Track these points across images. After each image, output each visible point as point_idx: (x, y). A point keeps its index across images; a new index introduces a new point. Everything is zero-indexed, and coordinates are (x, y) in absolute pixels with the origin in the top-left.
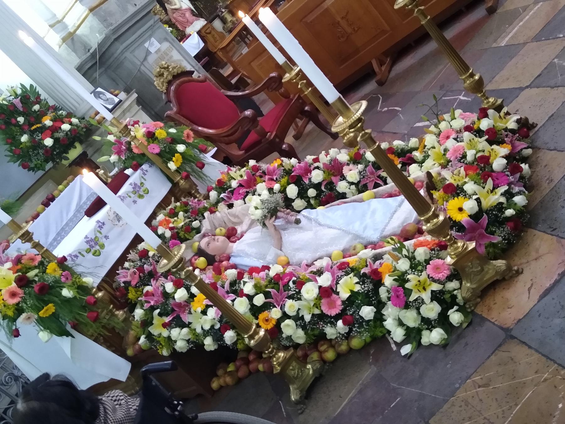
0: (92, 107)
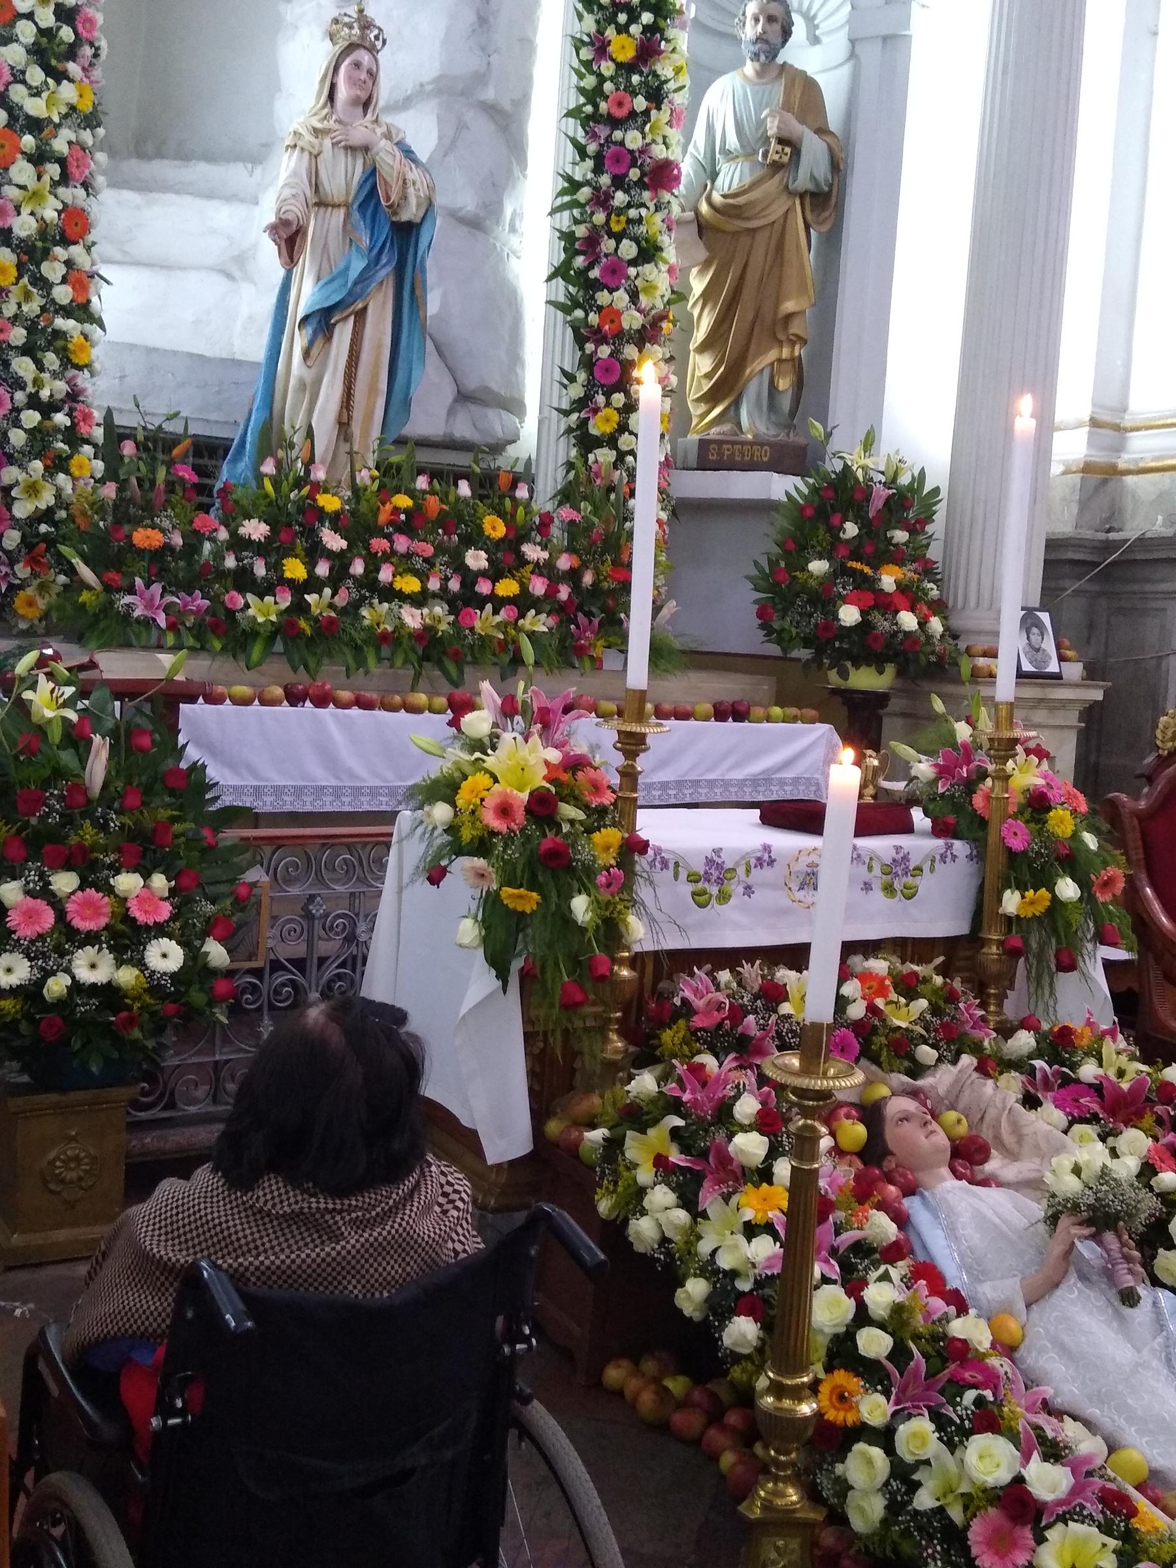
0: (996, 634)
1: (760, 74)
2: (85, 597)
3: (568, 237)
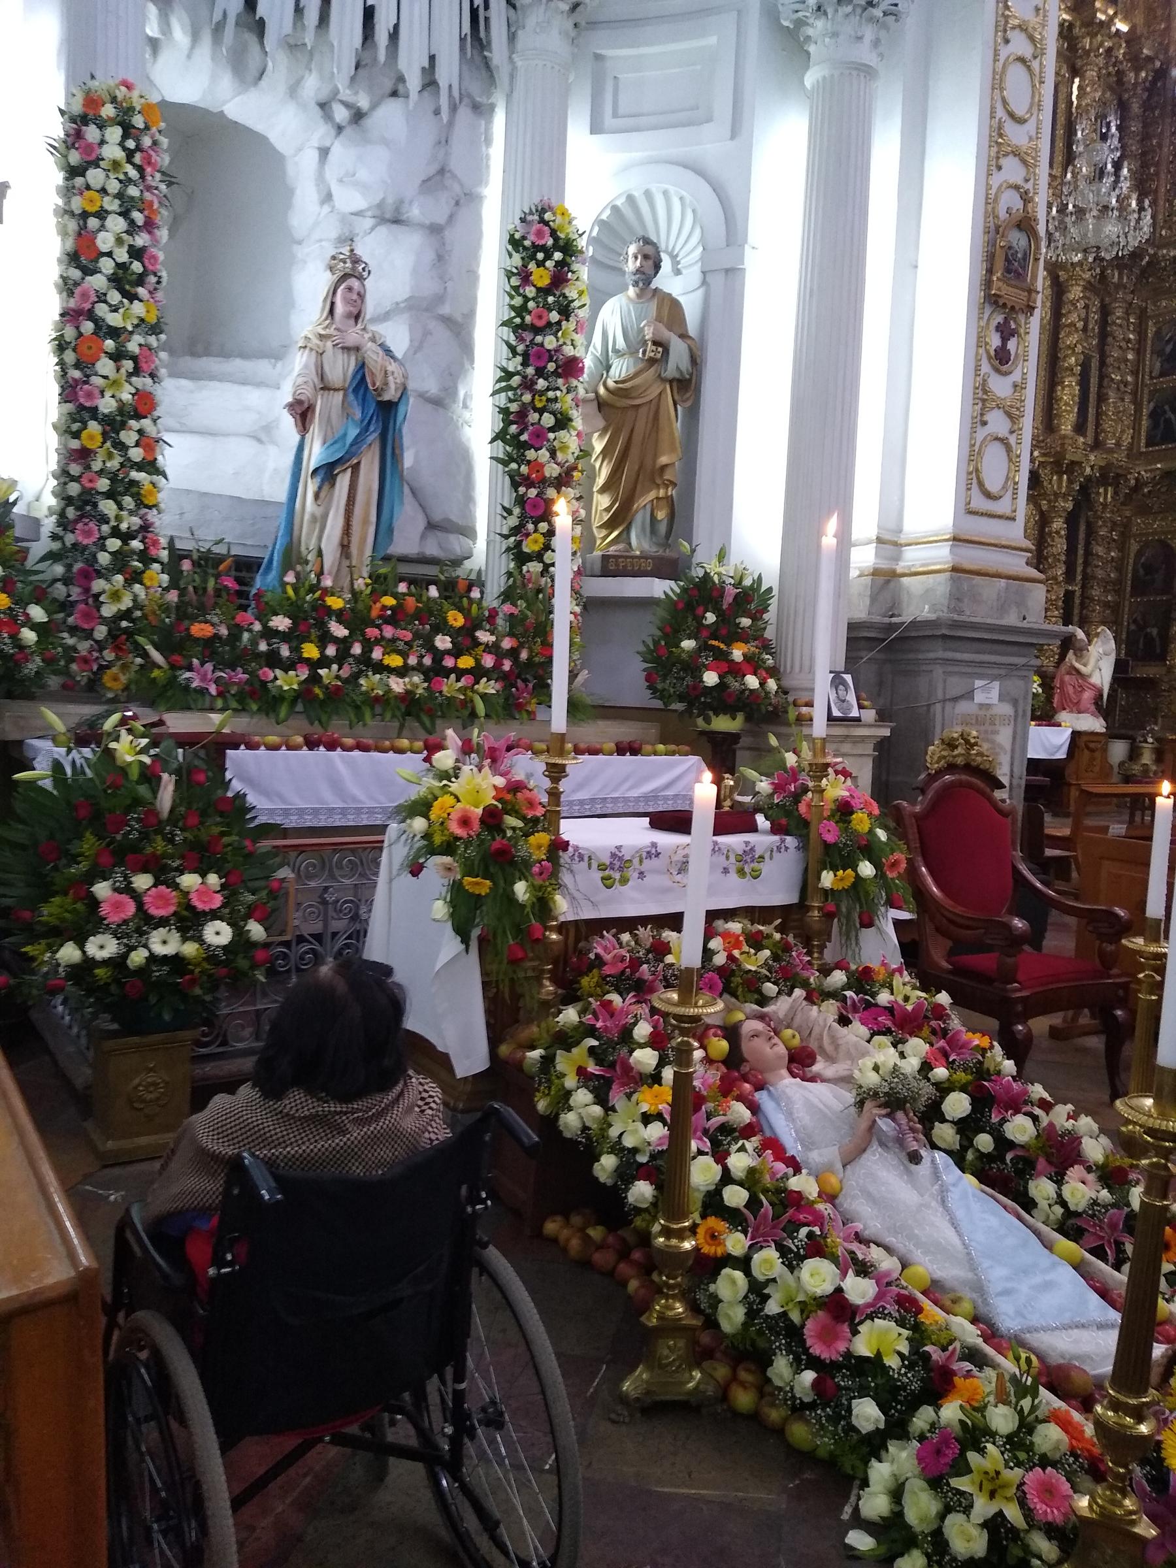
0: (812, 690)
2: (156, 673)
3: (504, 411)
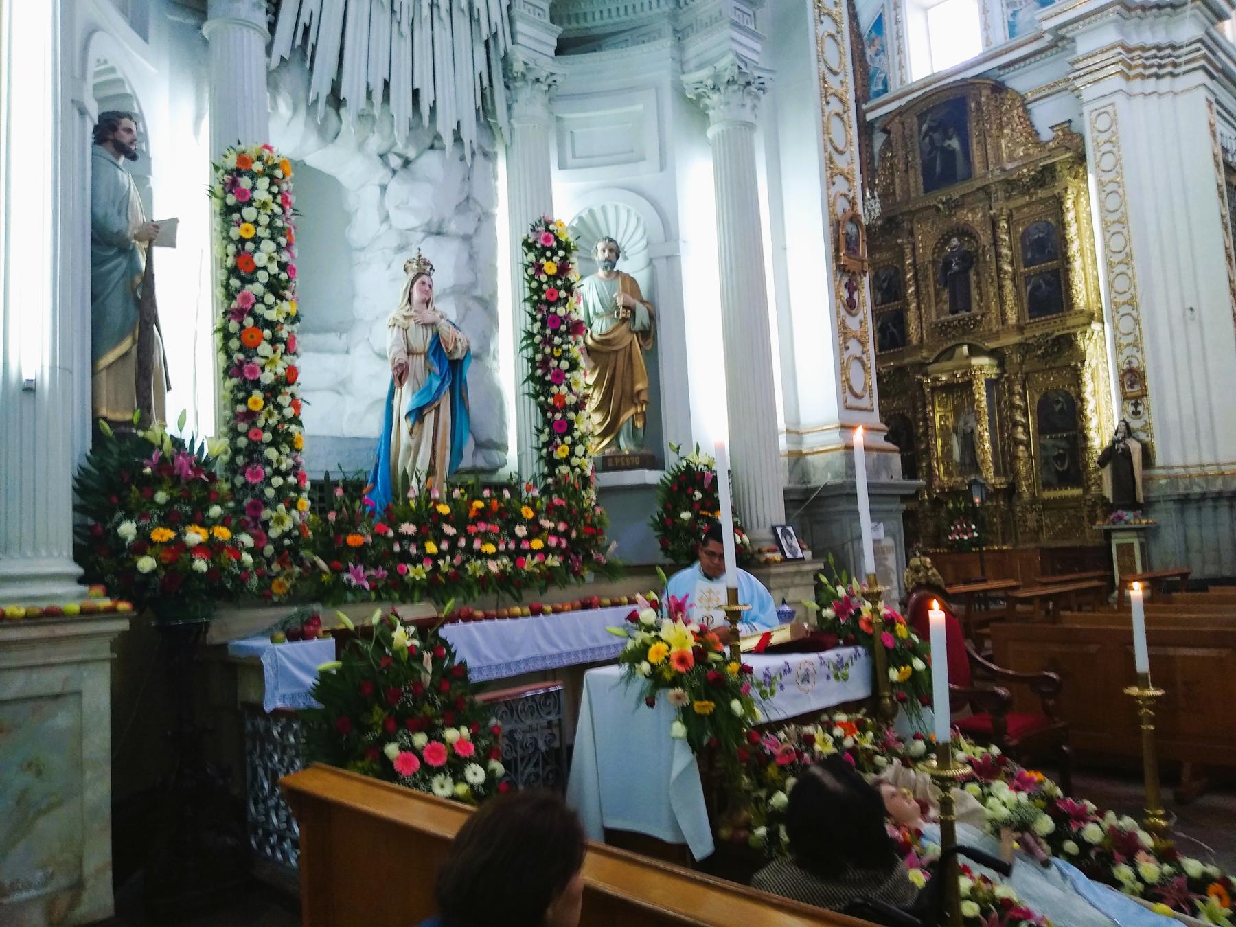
1: (608, 275)
3: (531, 360)
